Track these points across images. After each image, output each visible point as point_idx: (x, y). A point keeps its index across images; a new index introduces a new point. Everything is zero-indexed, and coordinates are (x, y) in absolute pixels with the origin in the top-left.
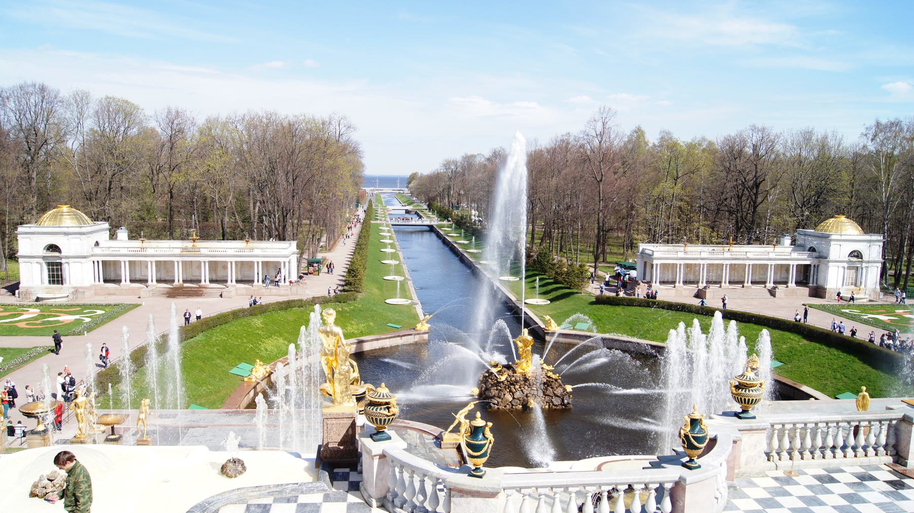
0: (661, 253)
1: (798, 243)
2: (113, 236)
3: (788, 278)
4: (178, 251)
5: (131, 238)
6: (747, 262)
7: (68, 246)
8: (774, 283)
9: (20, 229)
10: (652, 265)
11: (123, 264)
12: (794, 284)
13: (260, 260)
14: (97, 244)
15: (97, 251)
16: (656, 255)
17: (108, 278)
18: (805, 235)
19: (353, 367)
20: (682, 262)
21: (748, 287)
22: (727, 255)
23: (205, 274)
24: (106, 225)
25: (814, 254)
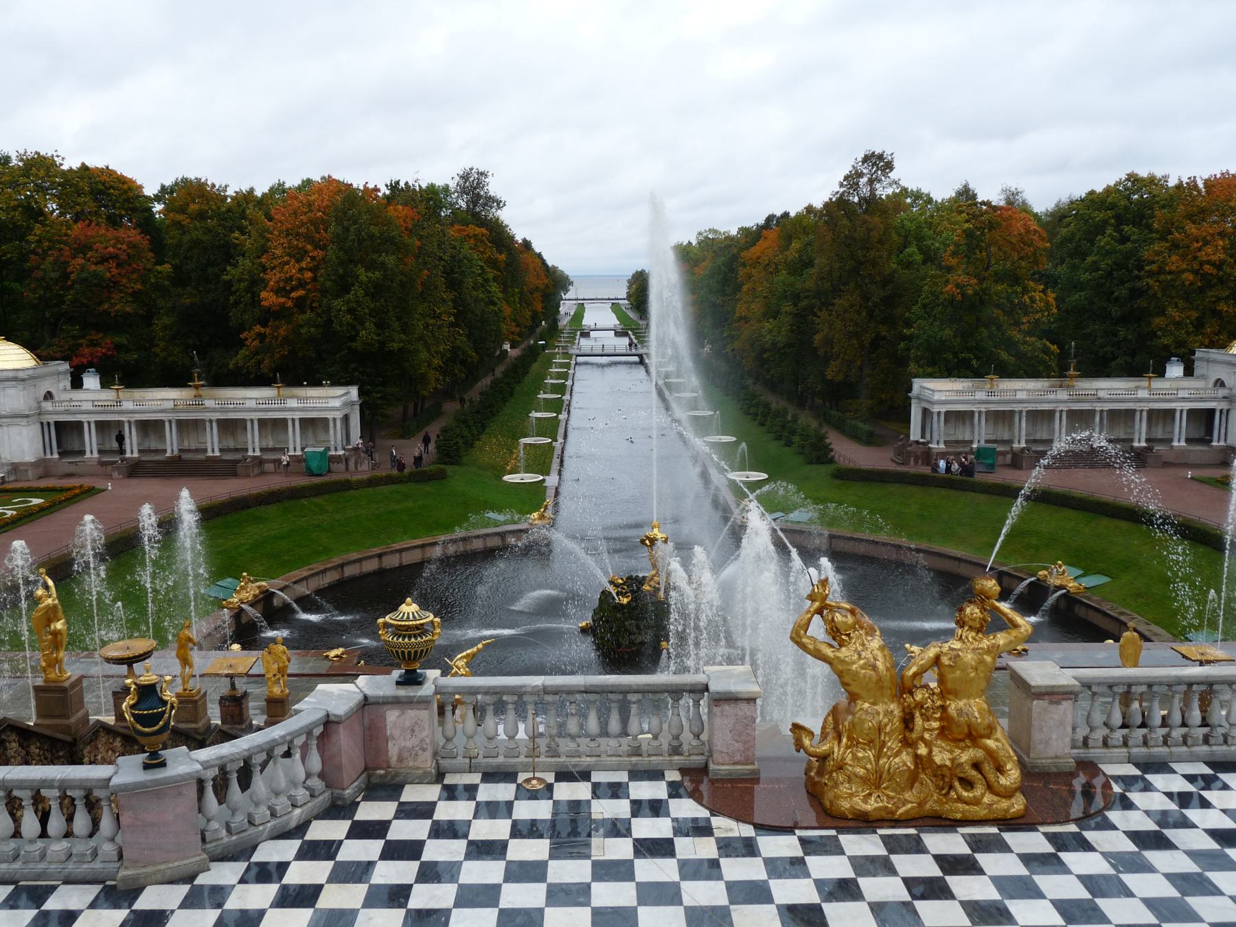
1: (1197, 372)
2: (77, 384)
3: (1172, 432)
4: (170, 405)
5: (105, 384)
6: (1098, 407)
8: (1148, 440)
11: (86, 425)
12: (1183, 444)
14: (49, 396)
15: (48, 406)
17: (69, 448)
18: (1208, 361)
19: (47, 587)
24: (65, 366)
25: (1222, 392)
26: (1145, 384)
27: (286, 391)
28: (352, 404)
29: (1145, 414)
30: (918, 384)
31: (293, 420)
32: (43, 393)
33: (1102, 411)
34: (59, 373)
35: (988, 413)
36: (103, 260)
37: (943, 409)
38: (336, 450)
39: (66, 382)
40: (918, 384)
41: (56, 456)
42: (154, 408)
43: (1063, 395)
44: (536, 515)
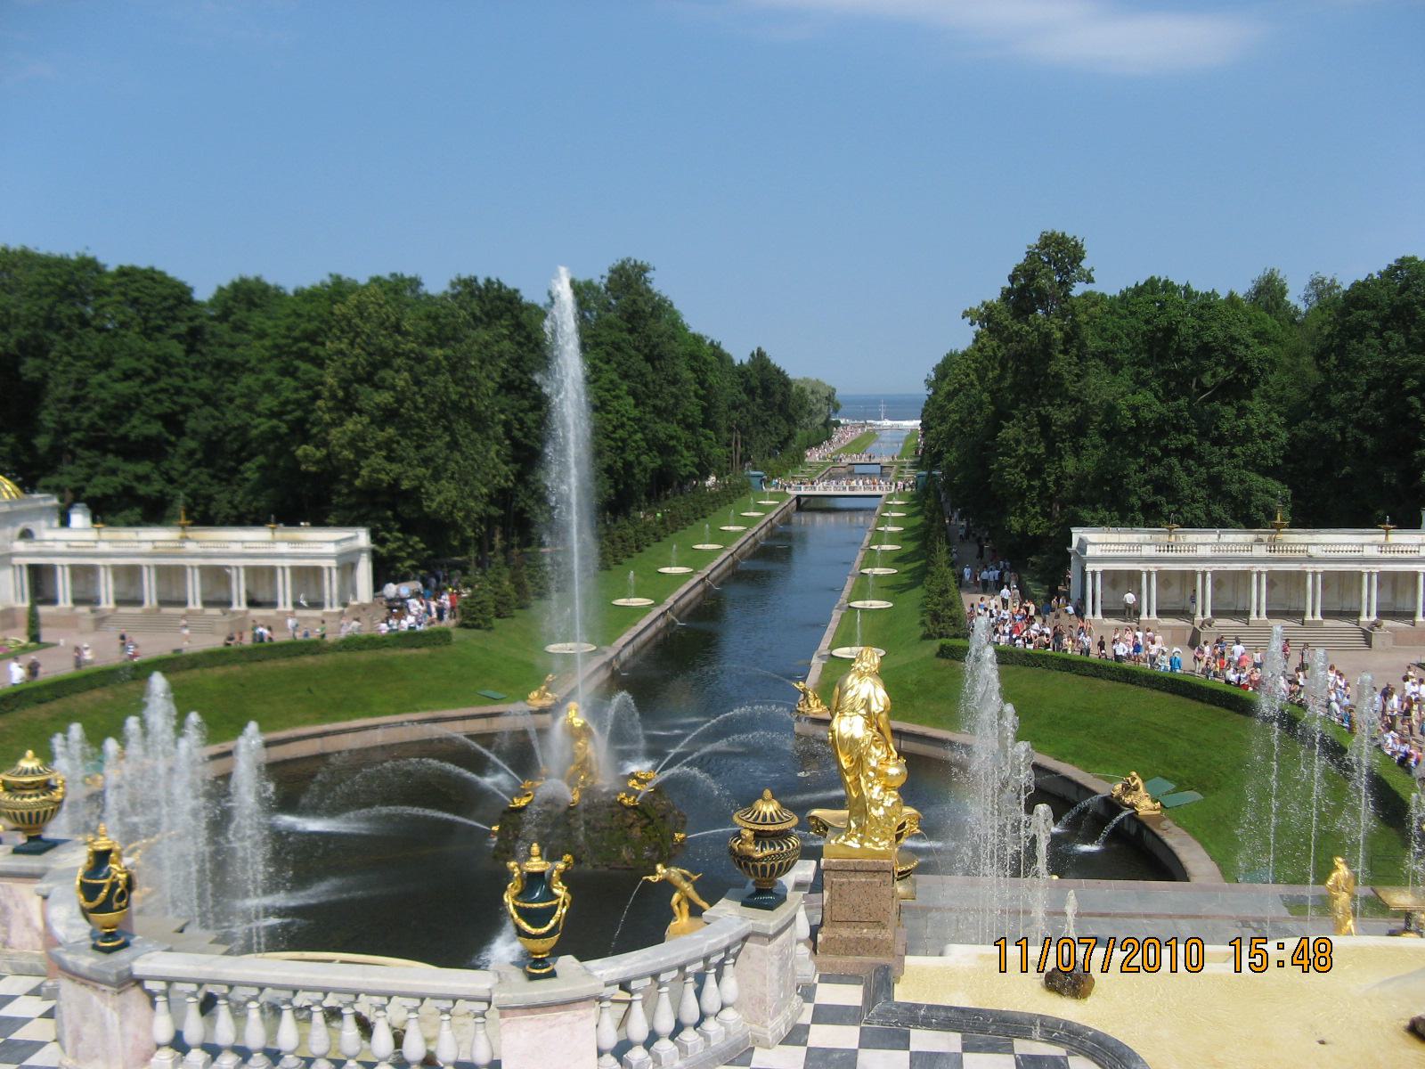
0: (1102, 546)
2: (65, 522)
4: (147, 547)
6: (1309, 568)
10: (1084, 574)
13: (287, 563)
15: (20, 546)
16: (1090, 551)
20: (1152, 567)
21: (1314, 624)
22: (1261, 551)
23: (194, 589)
26: (1381, 538)
27: (278, 535)
28: (360, 551)
29: (1375, 578)
30: (1077, 534)
31: (283, 568)
32: (18, 530)
33: (1314, 574)
35: (1160, 573)
36: (127, 376)
37: (1099, 567)
38: (331, 605)
40: (1077, 534)
42: (131, 550)
43: (1261, 551)
44: (536, 694)
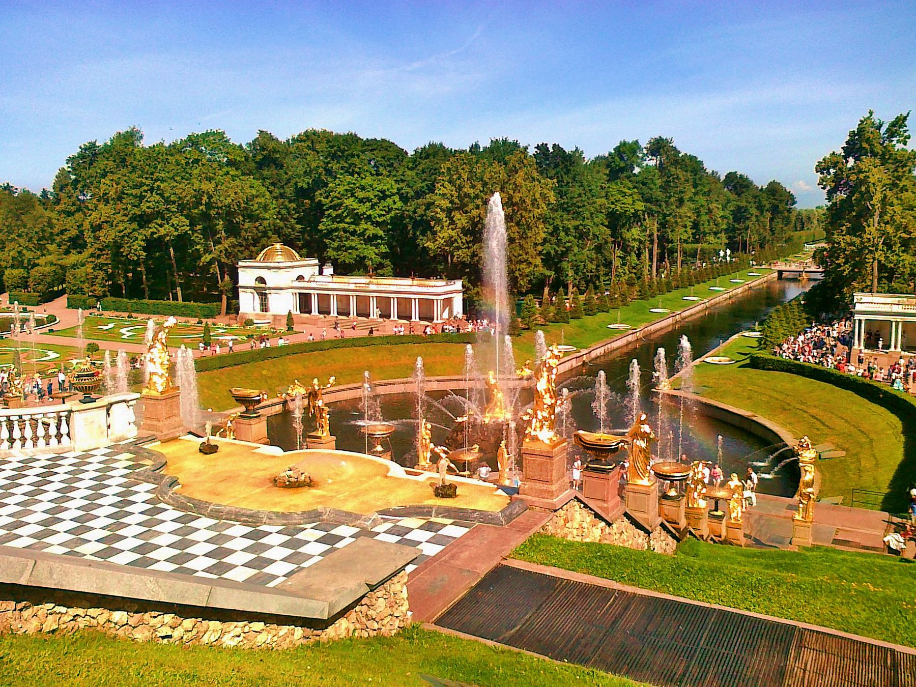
0: (869, 304)
2: (321, 273)
4: (352, 287)
7: (272, 278)
9: (240, 264)
14: (300, 278)
34: (309, 265)
39: (317, 273)
41: (298, 312)
